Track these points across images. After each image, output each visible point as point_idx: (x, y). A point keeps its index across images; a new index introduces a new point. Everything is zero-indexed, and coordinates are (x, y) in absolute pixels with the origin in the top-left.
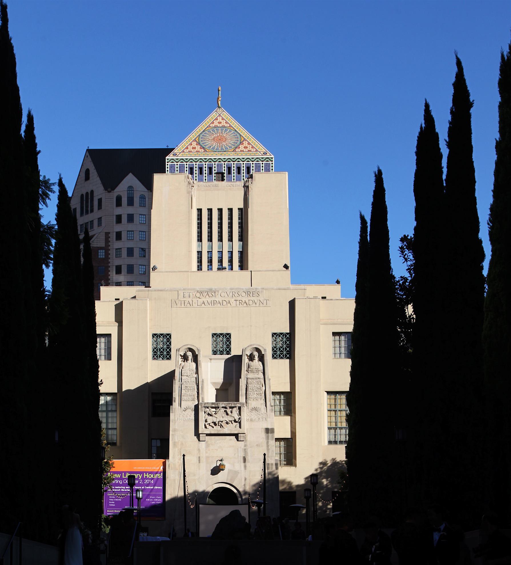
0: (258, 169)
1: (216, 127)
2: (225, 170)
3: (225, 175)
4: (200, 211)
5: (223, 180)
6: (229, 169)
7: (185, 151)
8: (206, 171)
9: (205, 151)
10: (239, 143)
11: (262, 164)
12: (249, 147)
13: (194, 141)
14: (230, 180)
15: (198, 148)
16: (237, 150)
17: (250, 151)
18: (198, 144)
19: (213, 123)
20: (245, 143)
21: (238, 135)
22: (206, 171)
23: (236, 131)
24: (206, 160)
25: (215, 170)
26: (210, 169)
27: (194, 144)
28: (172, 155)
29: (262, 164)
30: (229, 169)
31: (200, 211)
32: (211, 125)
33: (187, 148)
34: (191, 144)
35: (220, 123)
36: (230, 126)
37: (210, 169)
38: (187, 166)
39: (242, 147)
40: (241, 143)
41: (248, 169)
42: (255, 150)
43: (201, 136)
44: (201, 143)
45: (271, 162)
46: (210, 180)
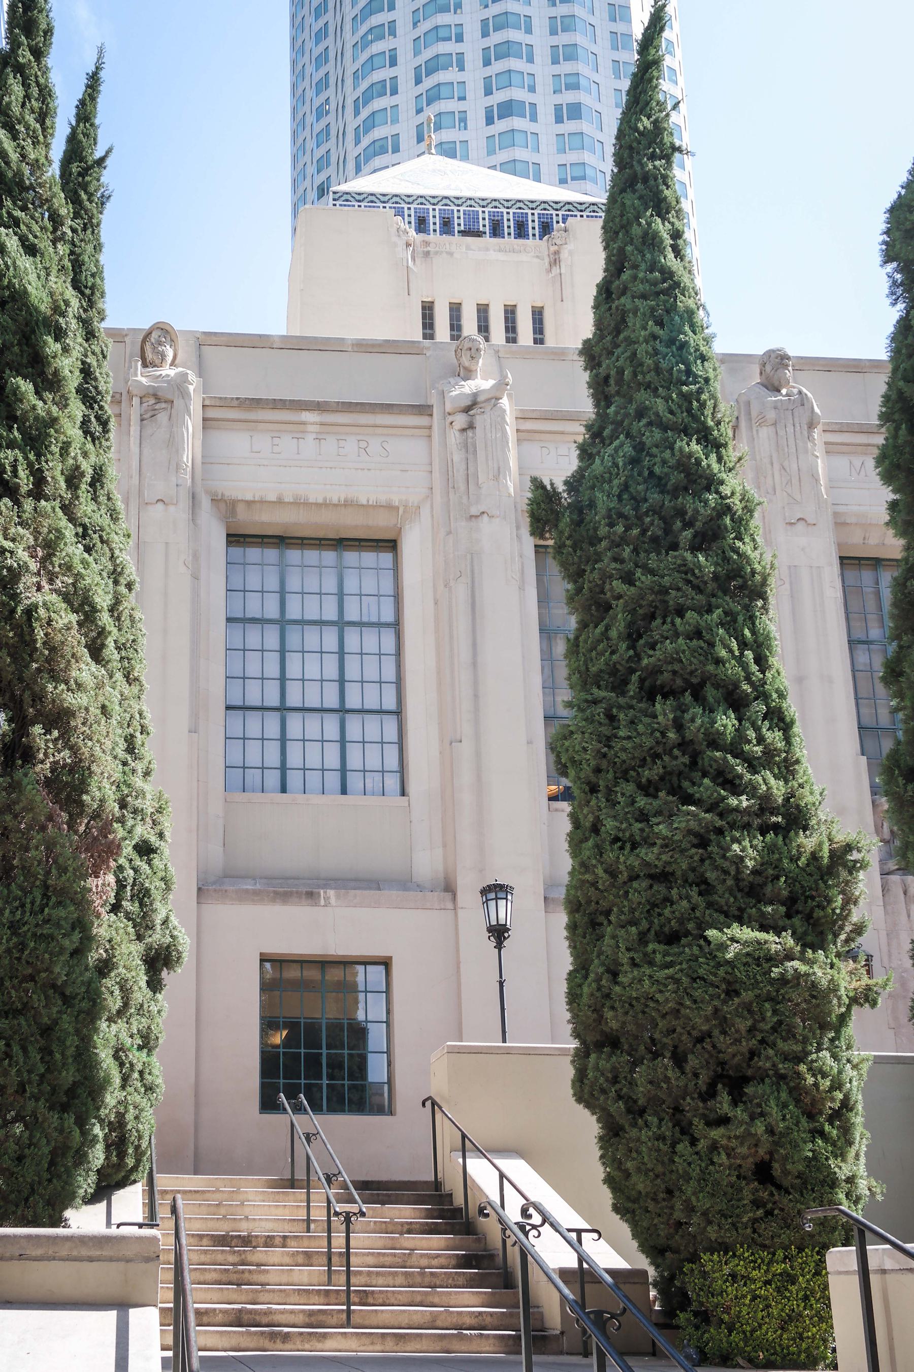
2: (484, 224)
25: (459, 223)
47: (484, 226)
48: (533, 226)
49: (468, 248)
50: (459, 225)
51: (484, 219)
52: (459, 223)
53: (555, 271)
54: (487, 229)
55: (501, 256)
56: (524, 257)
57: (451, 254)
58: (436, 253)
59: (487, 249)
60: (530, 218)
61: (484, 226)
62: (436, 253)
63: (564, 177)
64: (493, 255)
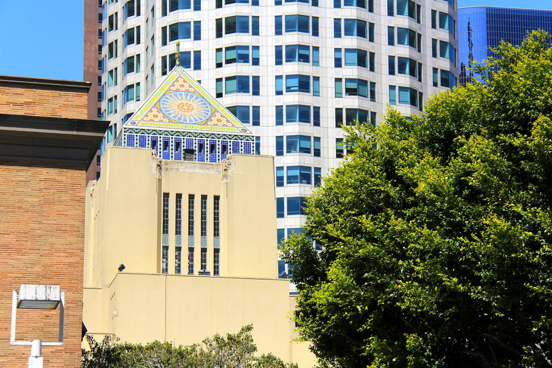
1: (177, 90)
3: (197, 153)
6: (201, 146)
7: (145, 119)
9: (170, 121)
10: (210, 114)
12: (224, 122)
13: (153, 107)
16: (209, 123)
18: (160, 111)
19: (173, 85)
21: (208, 105)
23: (203, 98)
25: (184, 146)
26: (178, 145)
27: (155, 111)
28: (129, 124)
30: (201, 146)
31: (166, 195)
32: (172, 88)
33: (147, 116)
34: (151, 111)
35: (182, 86)
36: (195, 91)
37: (178, 145)
40: (213, 115)
41: (224, 148)
42: (231, 125)
43: (162, 101)
44: (163, 110)
45: (252, 142)
46: (178, 158)
47: (196, 147)
49: (186, 167)
50: (184, 146)
51: (195, 143)
52: (184, 146)
53: (225, 181)
54: (197, 149)
55: (201, 171)
56: (212, 172)
57: (178, 169)
58: (171, 169)
59: (195, 167)
60: (217, 143)
61: (196, 147)
62: (171, 169)
63: (255, 51)
64: (197, 170)
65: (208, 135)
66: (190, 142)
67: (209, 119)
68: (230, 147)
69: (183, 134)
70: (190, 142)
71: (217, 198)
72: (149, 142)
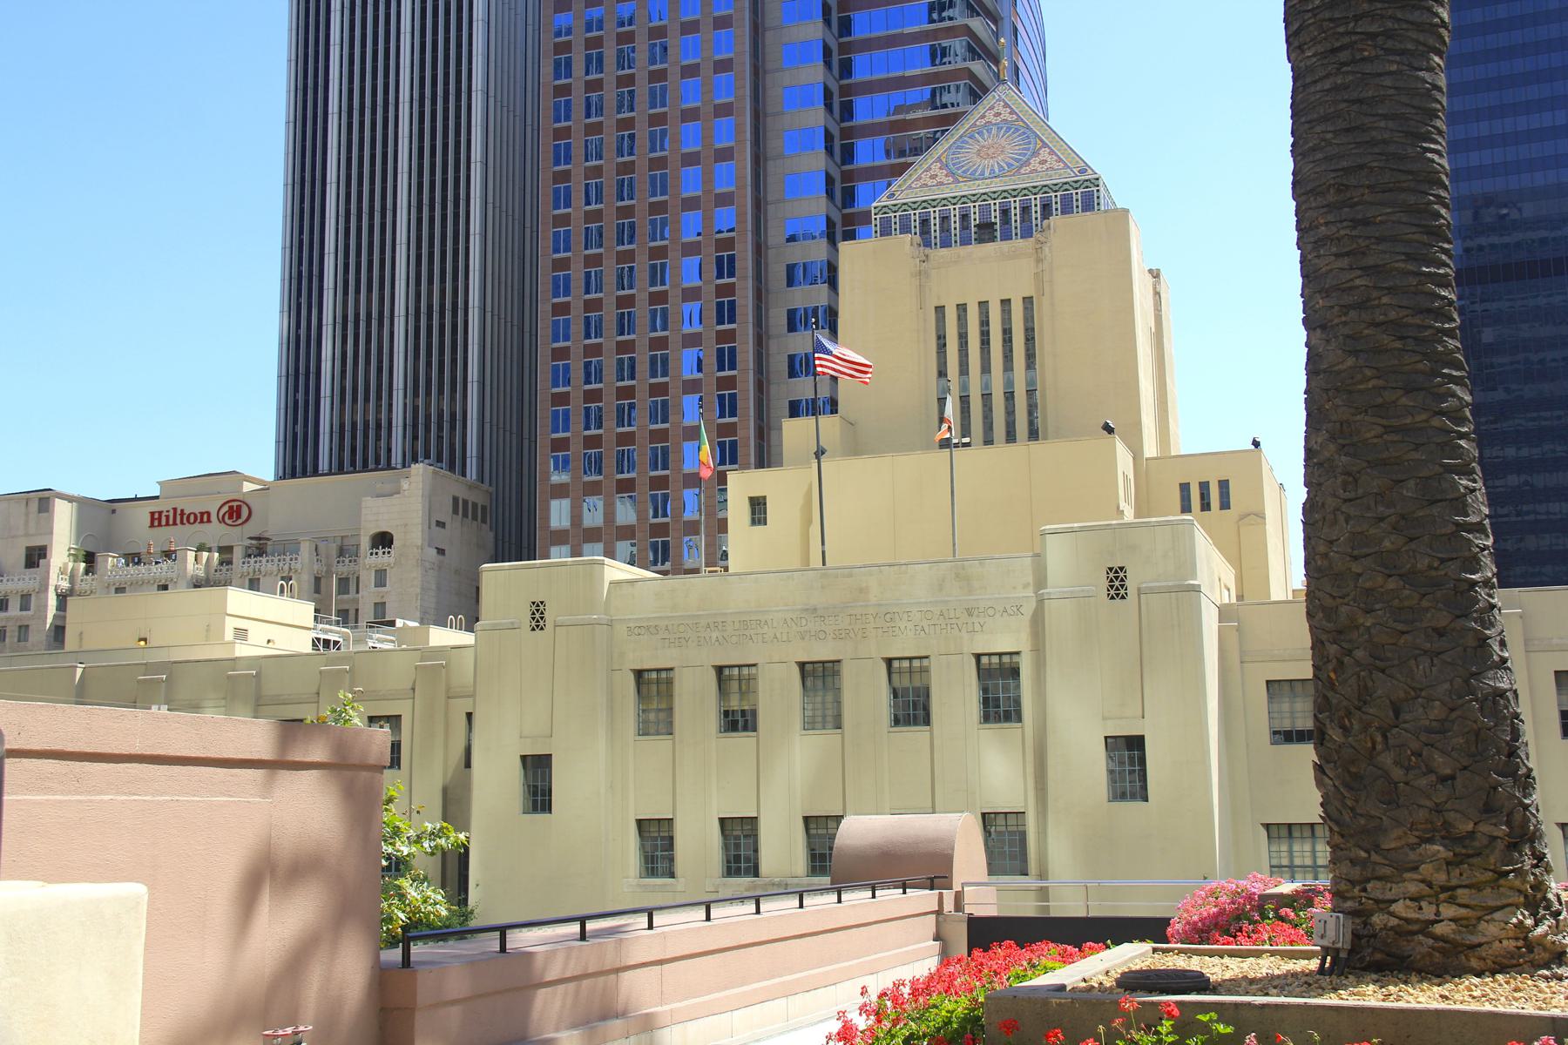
0: (1067, 209)
2: (995, 217)
4: (940, 310)
5: (993, 239)
6: (1005, 212)
8: (955, 223)
11: (1077, 195)
14: (1007, 236)
15: (941, 174)
17: (941, 184)
18: (945, 166)
20: (1044, 153)
22: (955, 223)
23: (1028, 127)
24: (954, 200)
25: (975, 219)
26: (965, 217)
29: (1077, 195)
30: (1005, 212)
31: (940, 310)
37: (965, 217)
38: (915, 217)
39: (1035, 162)
40: (1035, 153)
41: (1046, 209)
46: (965, 242)
48: (1036, 212)
52: (975, 219)
65: (1014, 193)
66: (985, 210)
67: (1027, 163)
68: (1056, 206)
69: (974, 198)
70: (985, 210)
71: (1028, 301)
72: (915, 224)
